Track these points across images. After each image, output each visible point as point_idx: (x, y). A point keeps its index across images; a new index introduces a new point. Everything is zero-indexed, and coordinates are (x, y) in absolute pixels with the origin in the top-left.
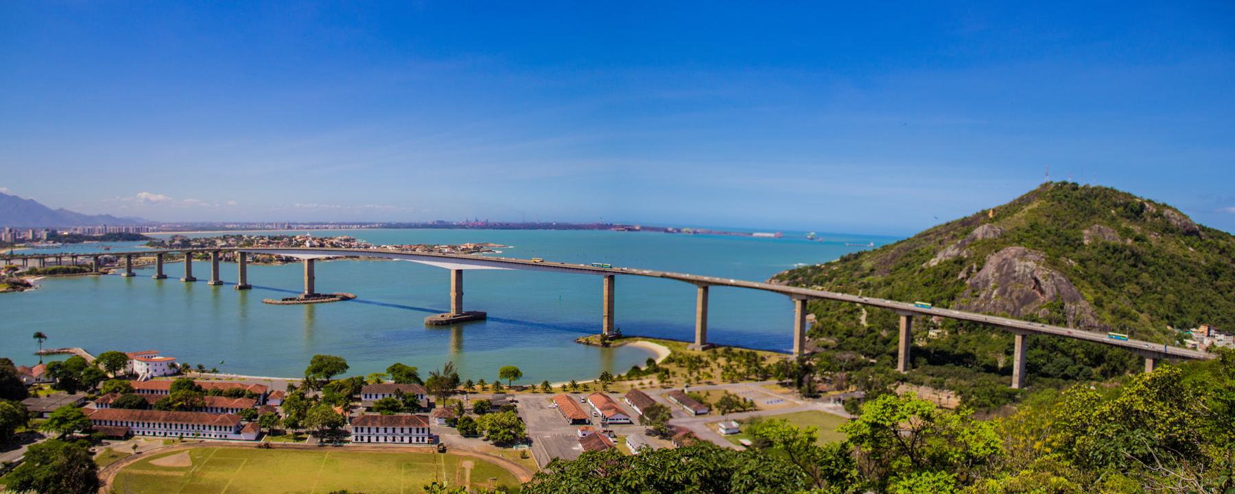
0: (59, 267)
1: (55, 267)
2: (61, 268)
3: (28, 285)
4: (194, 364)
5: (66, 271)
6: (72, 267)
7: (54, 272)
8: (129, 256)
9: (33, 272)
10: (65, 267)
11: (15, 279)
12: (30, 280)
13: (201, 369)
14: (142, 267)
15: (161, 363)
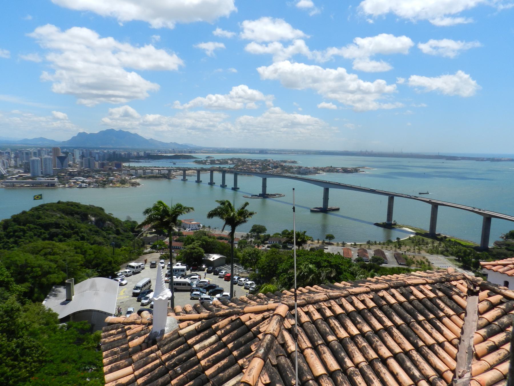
0: (152, 175)
1: (151, 175)
2: (153, 176)
3: (139, 184)
4: (207, 226)
5: (156, 177)
6: (158, 175)
7: (150, 178)
8: (184, 170)
9: (140, 177)
10: (155, 175)
11: (133, 181)
12: (138, 181)
13: (209, 227)
14: (191, 176)
15: (195, 224)
